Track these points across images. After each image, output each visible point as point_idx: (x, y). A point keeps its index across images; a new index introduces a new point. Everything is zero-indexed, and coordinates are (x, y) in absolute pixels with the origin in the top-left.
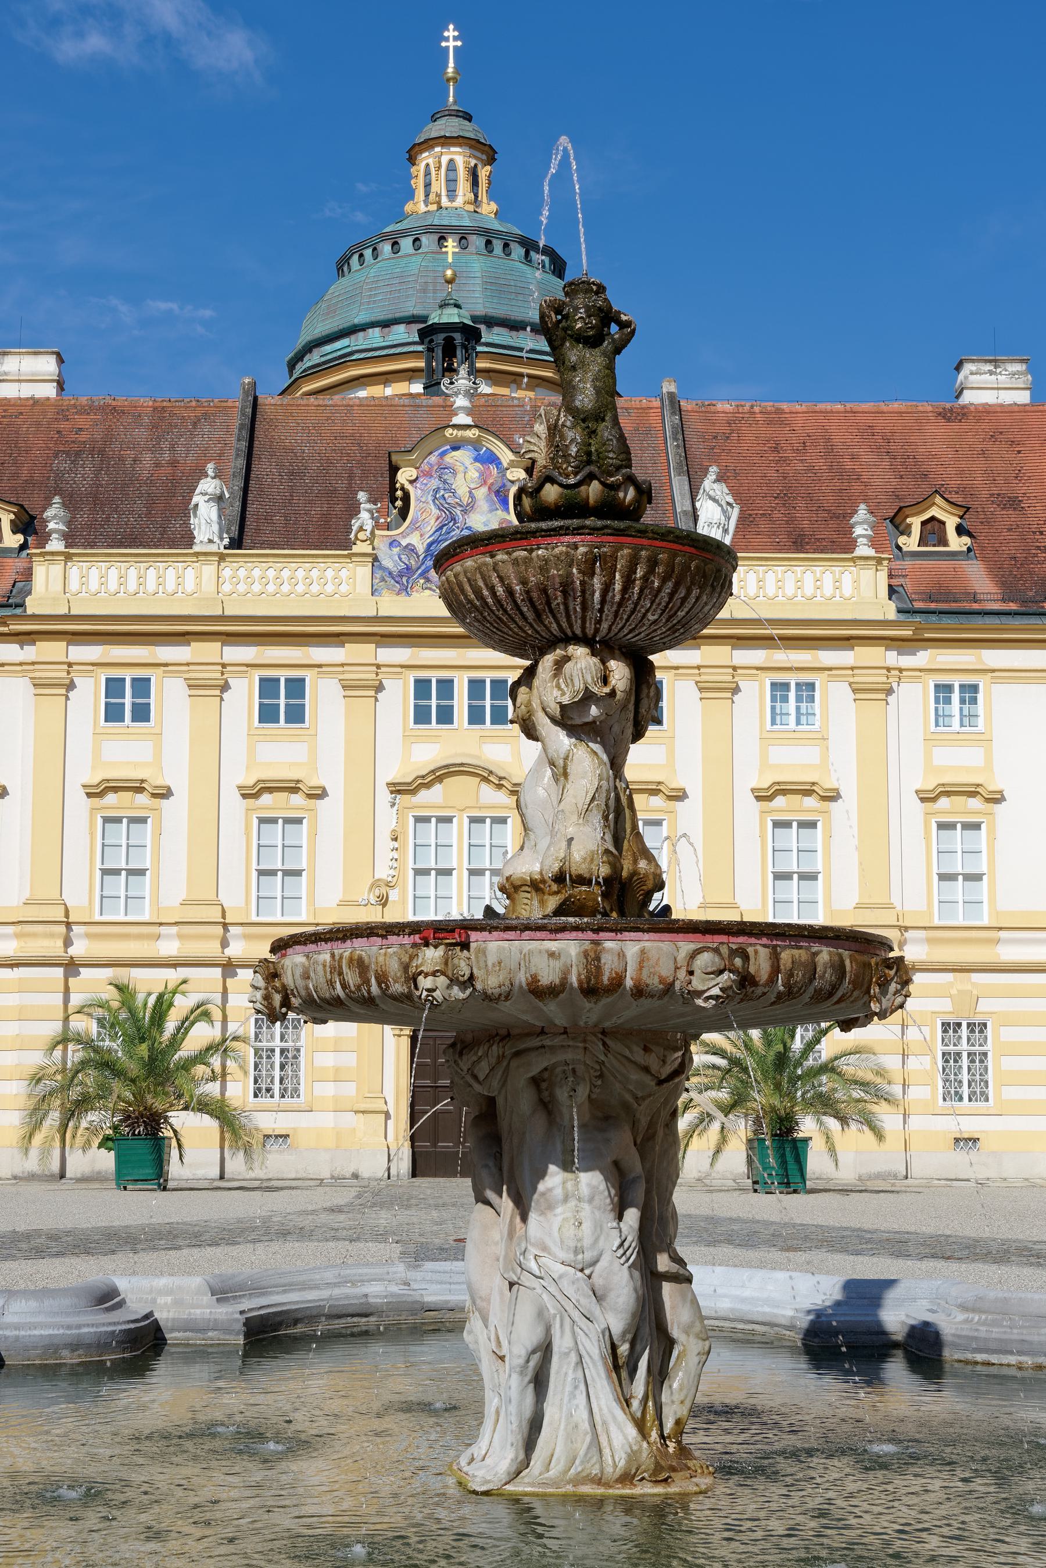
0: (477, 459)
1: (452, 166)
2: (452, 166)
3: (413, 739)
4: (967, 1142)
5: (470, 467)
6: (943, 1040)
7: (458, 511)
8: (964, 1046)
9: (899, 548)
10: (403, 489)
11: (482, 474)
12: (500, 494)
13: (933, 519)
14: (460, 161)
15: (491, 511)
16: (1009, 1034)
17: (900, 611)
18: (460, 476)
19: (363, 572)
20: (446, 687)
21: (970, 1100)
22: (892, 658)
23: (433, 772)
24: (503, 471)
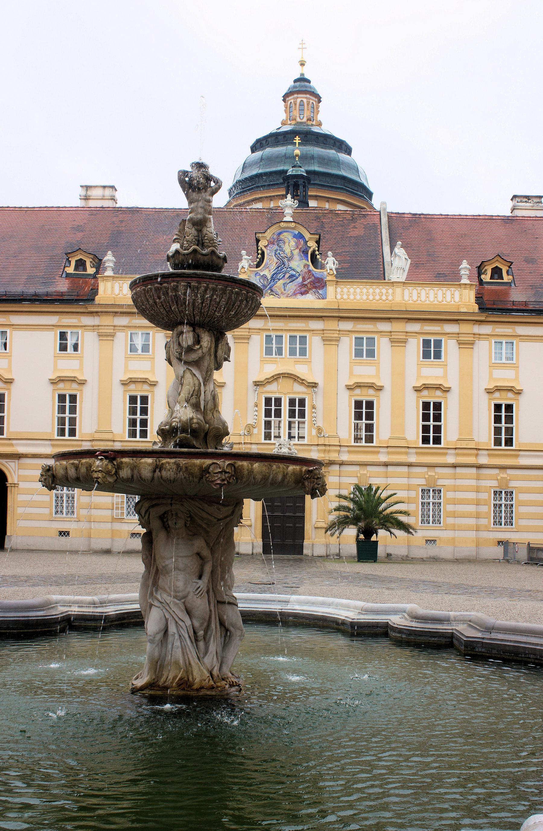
0: (294, 237)
1: (302, 104)
2: (302, 104)
3: (265, 362)
5: (291, 240)
6: (494, 499)
7: (286, 260)
8: (503, 502)
9: (482, 280)
10: (261, 250)
11: (296, 243)
12: (305, 252)
13: (497, 267)
14: (305, 100)
15: (300, 260)
16: (523, 497)
17: (479, 309)
18: (287, 244)
20: (279, 338)
21: (505, 525)
22: (477, 329)
23: (273, 376)
24: (306, 242)
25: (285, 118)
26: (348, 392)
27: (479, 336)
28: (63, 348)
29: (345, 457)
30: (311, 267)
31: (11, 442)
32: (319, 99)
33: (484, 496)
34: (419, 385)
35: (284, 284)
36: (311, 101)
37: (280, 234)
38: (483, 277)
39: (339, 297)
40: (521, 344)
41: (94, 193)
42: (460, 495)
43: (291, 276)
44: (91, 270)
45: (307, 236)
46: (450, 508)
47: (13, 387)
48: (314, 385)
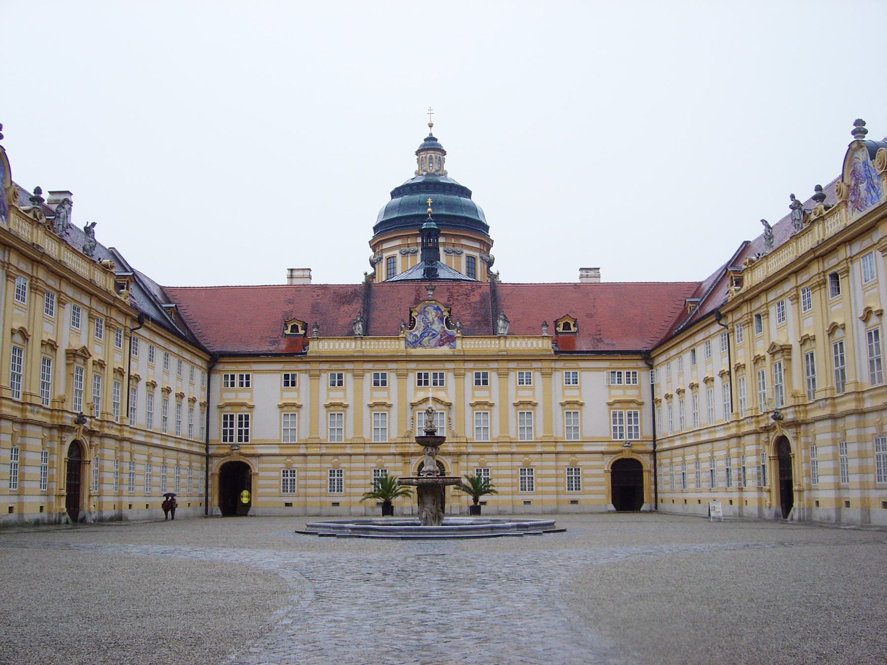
1: (431, 158)
2: (431, 158)
4: (574, 502)
7: (429, 324)
11: (436, 313)
12: (442, 319)
13: (566, 322)
14: (433, 155)
16: (586, 472)
19: (403, 342)
20: (426, 376)
22: (553, 365)
25: (417, 169)
26: (471, 408)
27: (556, 369)
28: (287, 384)
29: (470, 450)
30: (446, 329)
31: (253, 446)
32: (444, 153)
33: (561, 472)
34: (517, 402)
35: (429, 340)
36: (439, 156)
37: (425, 307)
38: (558, 329)
39: (464, 347)
40: (582, 373)
41: (295, 273)
42: (545, 472)
43: (434, 334)
44: (301, 332)
45: (443, 309)
46: (539, 480)
47: (255, 411)
48: (449, 405)
